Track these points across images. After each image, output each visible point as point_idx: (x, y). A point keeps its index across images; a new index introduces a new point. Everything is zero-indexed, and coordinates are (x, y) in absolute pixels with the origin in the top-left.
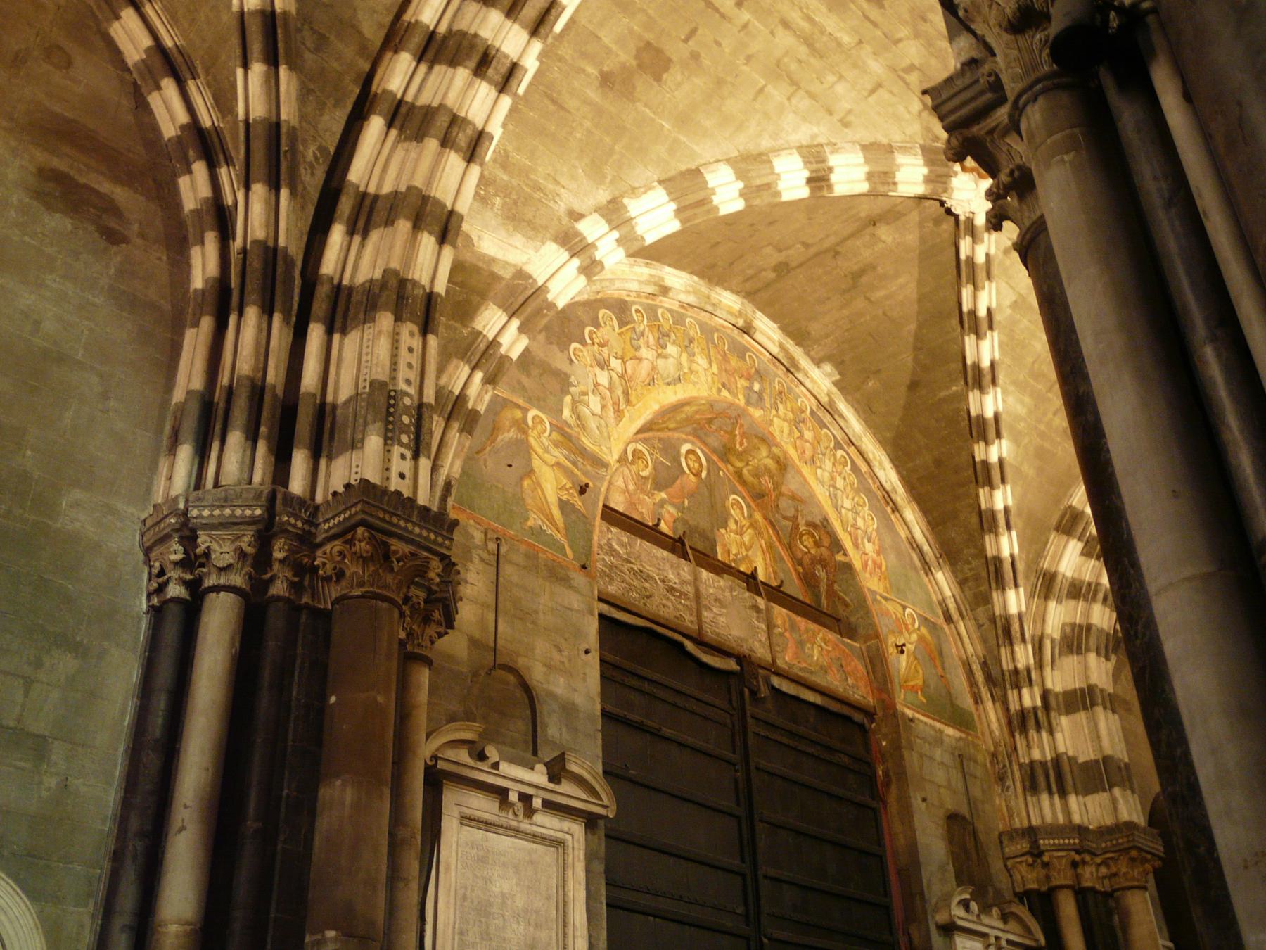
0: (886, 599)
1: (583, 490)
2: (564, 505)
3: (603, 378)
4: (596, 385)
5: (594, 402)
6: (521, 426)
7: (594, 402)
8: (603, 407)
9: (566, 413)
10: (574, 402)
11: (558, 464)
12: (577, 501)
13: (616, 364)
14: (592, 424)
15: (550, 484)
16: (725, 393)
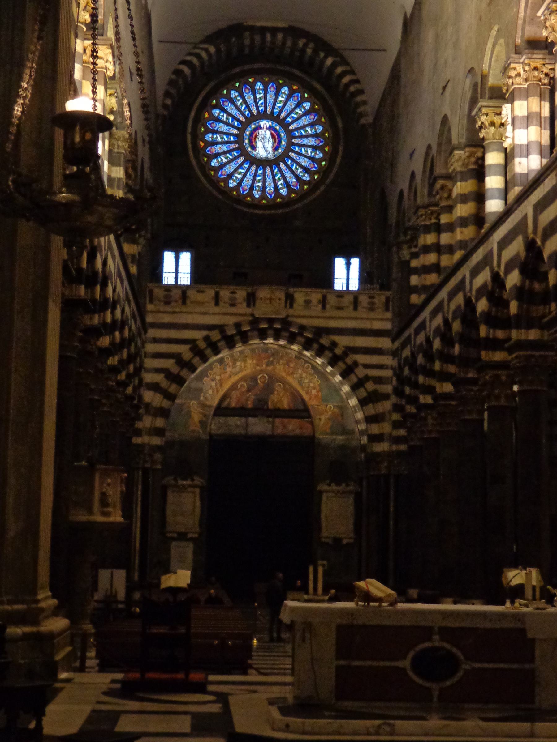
0: (318, 405)
1: (205, 416)
2: (200, 422)
3: (213, 384)
4: (211, 386)
5: (210, 392)
6: (189, 407)
7: (210, 392)
8: (213, 392)
9: (202, 398)
10: (205, 394)
11: (200, 412)
12: (204, 419)
13: (218, 378)
14: (210, 398)
15: (196, 417)
16: (258, 368)
